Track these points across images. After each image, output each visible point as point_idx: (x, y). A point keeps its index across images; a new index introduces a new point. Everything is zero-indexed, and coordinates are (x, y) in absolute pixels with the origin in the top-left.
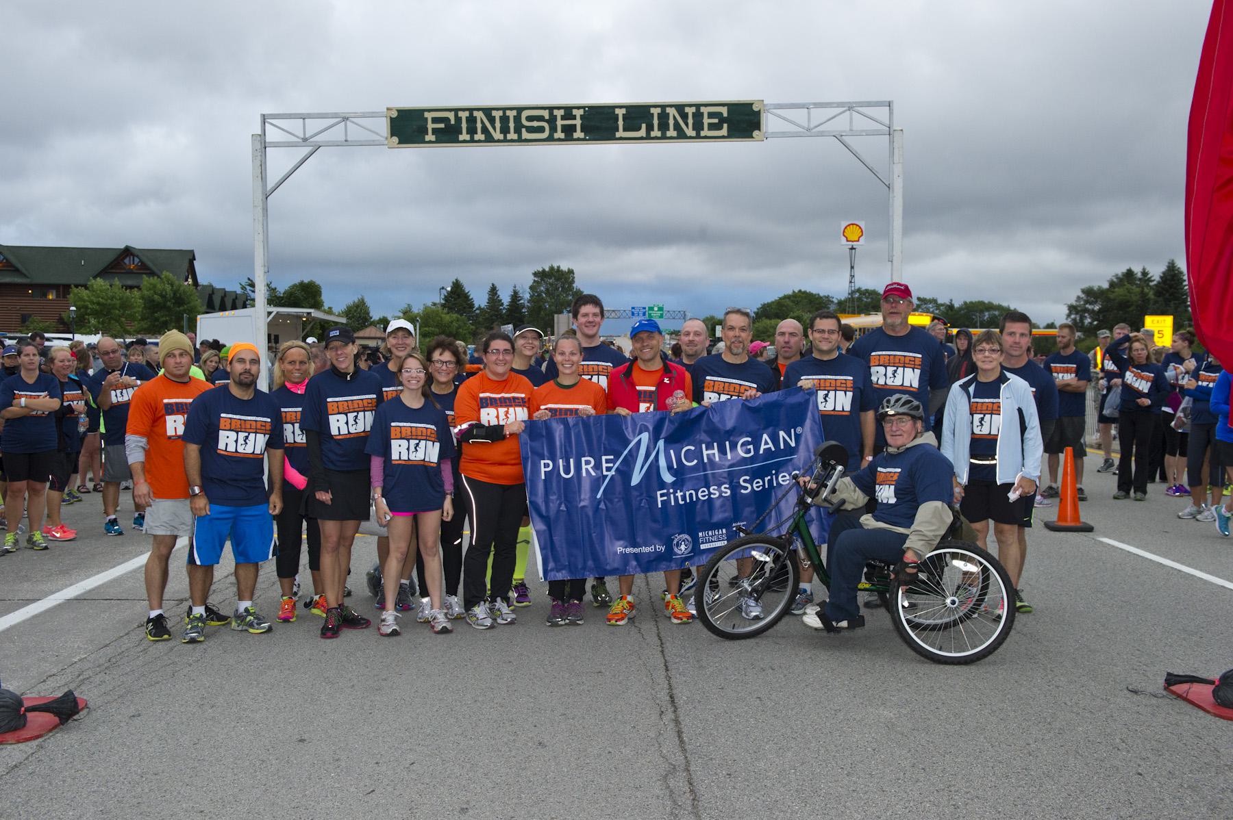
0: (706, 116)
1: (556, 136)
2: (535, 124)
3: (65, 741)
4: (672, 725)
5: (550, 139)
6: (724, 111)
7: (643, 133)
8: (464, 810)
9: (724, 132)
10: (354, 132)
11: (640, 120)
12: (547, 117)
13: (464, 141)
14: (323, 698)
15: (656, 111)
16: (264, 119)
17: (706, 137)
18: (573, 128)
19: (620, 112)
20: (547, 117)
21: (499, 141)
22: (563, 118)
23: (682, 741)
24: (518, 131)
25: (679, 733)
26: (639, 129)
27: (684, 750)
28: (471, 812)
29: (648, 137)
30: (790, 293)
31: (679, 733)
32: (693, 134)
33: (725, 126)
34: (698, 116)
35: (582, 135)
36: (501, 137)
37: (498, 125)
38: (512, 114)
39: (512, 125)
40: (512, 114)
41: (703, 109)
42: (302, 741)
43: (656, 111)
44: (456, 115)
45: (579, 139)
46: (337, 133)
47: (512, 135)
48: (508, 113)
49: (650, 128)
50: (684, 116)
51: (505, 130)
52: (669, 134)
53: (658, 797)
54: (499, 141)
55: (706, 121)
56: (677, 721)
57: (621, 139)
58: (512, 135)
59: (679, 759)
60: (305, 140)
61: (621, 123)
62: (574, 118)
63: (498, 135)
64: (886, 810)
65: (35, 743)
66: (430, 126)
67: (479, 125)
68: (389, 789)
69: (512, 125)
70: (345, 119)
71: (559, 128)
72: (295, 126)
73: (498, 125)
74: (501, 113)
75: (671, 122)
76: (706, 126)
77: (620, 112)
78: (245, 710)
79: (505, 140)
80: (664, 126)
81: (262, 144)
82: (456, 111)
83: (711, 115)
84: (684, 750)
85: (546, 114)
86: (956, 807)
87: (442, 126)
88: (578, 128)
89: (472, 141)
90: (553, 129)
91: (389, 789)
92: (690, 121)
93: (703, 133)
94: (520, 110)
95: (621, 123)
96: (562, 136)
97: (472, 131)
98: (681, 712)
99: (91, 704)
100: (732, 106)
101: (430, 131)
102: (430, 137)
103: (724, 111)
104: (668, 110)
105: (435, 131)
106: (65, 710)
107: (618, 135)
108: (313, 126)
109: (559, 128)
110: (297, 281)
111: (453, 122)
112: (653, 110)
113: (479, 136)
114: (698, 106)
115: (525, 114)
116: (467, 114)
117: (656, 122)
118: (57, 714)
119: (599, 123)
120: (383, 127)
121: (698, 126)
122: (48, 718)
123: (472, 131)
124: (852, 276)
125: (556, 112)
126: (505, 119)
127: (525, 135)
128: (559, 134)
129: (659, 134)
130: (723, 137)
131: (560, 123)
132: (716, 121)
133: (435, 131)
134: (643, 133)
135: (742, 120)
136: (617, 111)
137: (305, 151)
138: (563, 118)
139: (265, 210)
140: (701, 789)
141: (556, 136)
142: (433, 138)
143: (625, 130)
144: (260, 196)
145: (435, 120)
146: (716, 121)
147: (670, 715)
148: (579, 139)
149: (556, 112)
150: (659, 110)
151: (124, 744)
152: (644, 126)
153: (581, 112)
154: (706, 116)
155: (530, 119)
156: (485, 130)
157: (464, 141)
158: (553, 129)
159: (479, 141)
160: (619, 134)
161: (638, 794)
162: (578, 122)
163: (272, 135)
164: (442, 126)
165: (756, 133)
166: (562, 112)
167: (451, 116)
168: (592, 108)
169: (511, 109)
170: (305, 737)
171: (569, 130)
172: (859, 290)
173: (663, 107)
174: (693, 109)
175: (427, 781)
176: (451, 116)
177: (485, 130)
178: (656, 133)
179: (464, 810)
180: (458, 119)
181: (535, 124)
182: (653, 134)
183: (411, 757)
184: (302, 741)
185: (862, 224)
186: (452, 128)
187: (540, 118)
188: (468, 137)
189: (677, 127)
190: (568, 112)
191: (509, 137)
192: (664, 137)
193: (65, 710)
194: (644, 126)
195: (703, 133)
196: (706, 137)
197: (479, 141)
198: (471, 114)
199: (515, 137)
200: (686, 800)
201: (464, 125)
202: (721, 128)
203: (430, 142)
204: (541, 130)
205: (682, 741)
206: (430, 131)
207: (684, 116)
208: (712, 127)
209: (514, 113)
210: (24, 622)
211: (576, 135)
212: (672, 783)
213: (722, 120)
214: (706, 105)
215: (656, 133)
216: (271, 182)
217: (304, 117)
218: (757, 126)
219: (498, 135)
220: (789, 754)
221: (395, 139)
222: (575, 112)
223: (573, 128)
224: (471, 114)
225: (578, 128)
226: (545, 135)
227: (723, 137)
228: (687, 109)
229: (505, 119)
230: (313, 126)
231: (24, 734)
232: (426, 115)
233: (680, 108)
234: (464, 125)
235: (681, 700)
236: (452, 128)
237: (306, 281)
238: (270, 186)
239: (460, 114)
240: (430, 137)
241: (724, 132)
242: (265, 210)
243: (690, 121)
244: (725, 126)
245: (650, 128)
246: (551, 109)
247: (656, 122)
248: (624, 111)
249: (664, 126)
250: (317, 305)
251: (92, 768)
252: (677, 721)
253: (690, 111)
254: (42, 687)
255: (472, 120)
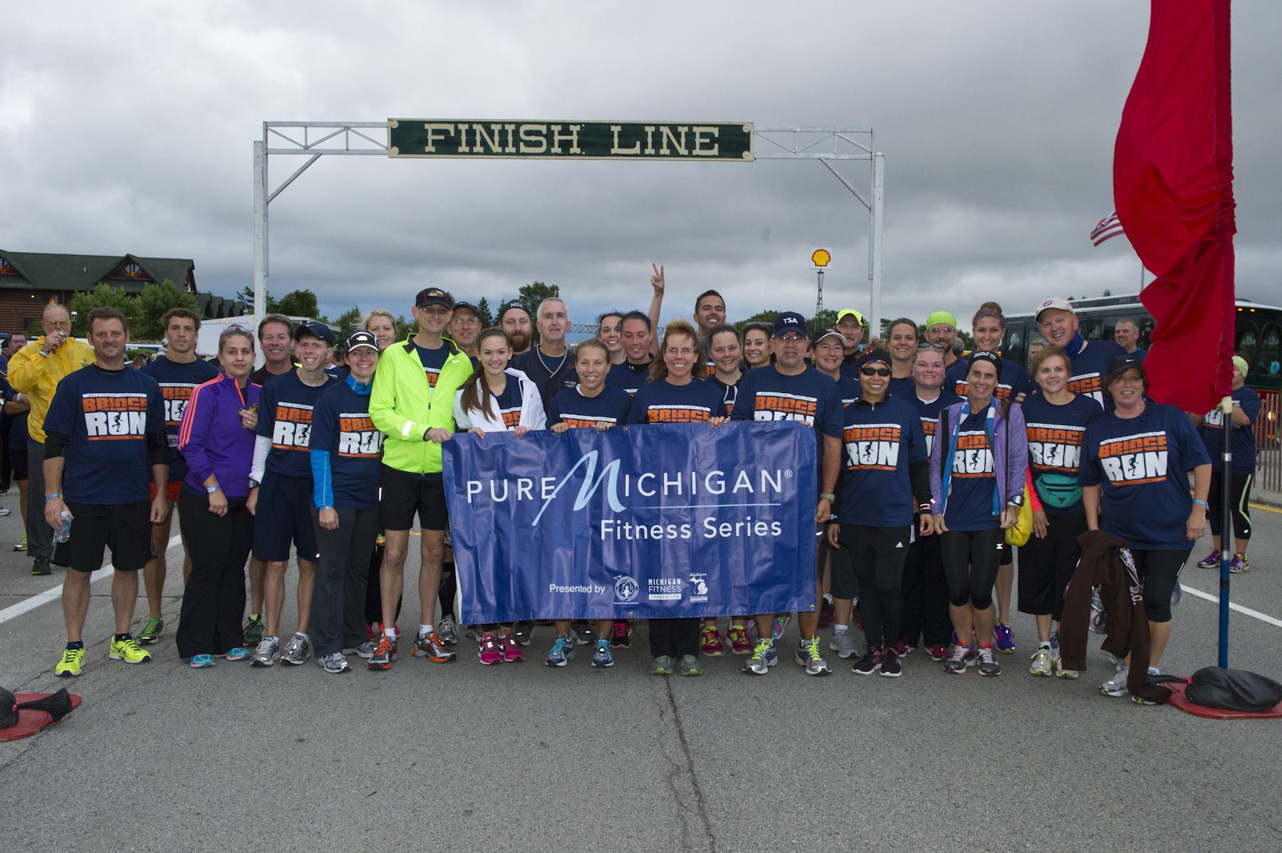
0: (698, 136)
1: (553, 150)
2: (533, 138)
3: (56, 739)
4: (673, 725)
5: (548, 153)
6: (716, 131)
7: (637, 150)
8: (468, 813)
9: (715, 151)
10: (356, 142)
11: (634, 136)
12: (545, 132)
13: (464, 153)
14: (321, 696)
15: (650, 130)
16: (267, 126)
17: (698, 156)
18: (570, 143)
19: (616, 130)
20: (545, 132)
21: (497, 154)
22: (560, 133)
23: (684, 741)
24: (516, 144)
25: (681, 733)
26: (634, 146)
27: (687, 751)
28: (475, 815)
29: (642, 154)
30: (762, 312)
31: (681, 733)
32: (686, 152)
33: (716, 146)
34: (691, 135)
35: (578, 151)
36: (500, 150)
37: (497, 138)
38: (510, 128)
39: (510, 139)
40: (510, 128)
41: (695, 129)
42: (301, 740)
43: (650, 130)
44: (456, 128)
45: (575, 154)
46: (338, 142)
47: (510, 149)
48: (507, 127)
49: (644, 146)
50: (677, 136)
51: (503, 144)
52: (662, 152)
53: (663, 798)
54: (497, 154)
55: (698, 140)
56: (677, 721)
57: (616, 155)
58: (510, 149)
59: (681, 759)
60: (306, 148)
61: (616, 140)
62: (571, 133)
63: (496, 148)
64: (889, 810)
65: (26, 741)
66: (431, 137)
67: (478, 138)
68: (391, 790)
69: (510, 139)
70: (347, 128)
71: (556, 143)
72: (297, 134)
73: (497, 138)
74: (499, 127)
75: (665, 140)
76: (698, 145)
77: (616, 130)
78: (243, 708)
79: (504, 153)
80: (657, 144)
81: (263, 151)
82: (456, 123)
83: (703, 135)
84: (687, 751)
85: (544, 129)
86: (957, 806)
87: (442, 137)
88: (575, 144)
89: (471, 153)
90: (551, 144)
91: (391, 790)
92: (683, 140)
93: (695, 152)
94: (518, 124)
95: (616, 140)
96: (559, 151)
97: (471, 143)
98: (681, 712)
99: (85, 701)
100: (722, 127)
101: (430, 143)
102: (430, 148)
103: (716, 131)
104: (662, 129)
105: (434, 142)
106: (57, 708)
107: (613, 151)
108: (315, 134)
109: (556, 143)
110: (293, 291)
111: (452, 134)
112: (647, 129)
113: (478, 149)
114: (691, 126)
115: (523, 128)
116: (467, 127)
117: (650, 140)
118: (50, 711)
119: (596, 139)
120: (383, 137)
121: (690, 145)
122: (40, 715)
123: (471, 143)
124: (820, 299)
125: (553, 128)
126: (503, 133)
127: (523, 149)
128: (556, 149)
129: (653, 152)
130: (714, 156)
131: (557, 138)
132: (708, 141)
133: (434, 142)
134: (637, 150)
135: (732, 141)
136: (613, 128)
137: (311, 156)
138: (560, 133)
139: (266, 215)
140: (706, 790)
141: (553, 150)
142: (433, 149)
143: (620, 146)
144: (261, 202)
145: (435, 132)
146: (708, 141)
147: (670, 715)
148: (575, 154)
149: (553, 128)
150: (653, 129)
151: (118, 743)
152: (638, 143)
153: (578, 128)
154: (698, 136)
155: (528, 133)
156: (484, 143)
157: (464, 153)
158: (551, 144)
159: (478, 153)
160: (615, 150)
161: (643, 795)
162: (575, 138)
163: (274, 142)
164: (442, 137)
165: (745, 154)
166: (559, 128)
167: (451, 128)
168: (587, 124)
169: (510, 123)
170: (304, 736)
171: (566, 146)
172: (825, 312)
173: (657, 126)
174: (686, 129)
175: (430, 782)
176: (451, 128)
177: (484, 143)
178: (650, 150)
179: (468, 813)
180: (458, 132)
181: (533, 138)
182: (647, 152)
183: (412, 757)
184: (301, 740)
185: (829, 250)
186: (452, 140)
187: (538, 133)
188: (467, 150)
189: (670, 145)
190: (565, 128)
191: (507, 150)
192: (657, 155)
193: (57, 708)
194: (638, 143)
195: (695, 152)
196: (698, 156)
197: (478, 153)
198: (471, 127)
199: (513, 150)
200: (692, 800)
201: (464, 138)
202: (712, 148)
203: (430, 153)
204: (539, 144)
205: (684, 741)
206: (430, 143)
207: (677, 136)
208: (703, 146)
209: (513, 127)
210: (19, 617)
211: (572, 151)
212: (676, 784)
213: (714, 140)
214: (698, 126)
215: (650, 150)
216: (272, 189)
217: (306, 125)
218: (747, 147)
219: (496, 148)
220: (790, 754)
221: (396, 149)
222: (572, 128)
223: (570, 143)
224: (471, 127)
225: (575, 144)
226: (543, 149)
227: (714, 156)
228: (680, 129)
229: (503, 133)
230: (315, 134)
231: (17, 731)
232: (427, 126)
233: (674, 128)
234: (464, 138)
235: (680, 700)
236: (452, 140)
237: (302, 290)
238: (271, 191)
239: (460, 126)
240: (430, 148)
241: (715, 151)
242: (266, 215)
243: (683, 140)
244: (716, 146)
245: (644, 146)
246: (549, 124)
247: (650, 140)
248: (619, 128)
249: (657, 144)
250: (313, 313)
251: (86, 767)
252: (677, 721)
253: (683, 130)
254: (36, 683)
255: (471, 133)
